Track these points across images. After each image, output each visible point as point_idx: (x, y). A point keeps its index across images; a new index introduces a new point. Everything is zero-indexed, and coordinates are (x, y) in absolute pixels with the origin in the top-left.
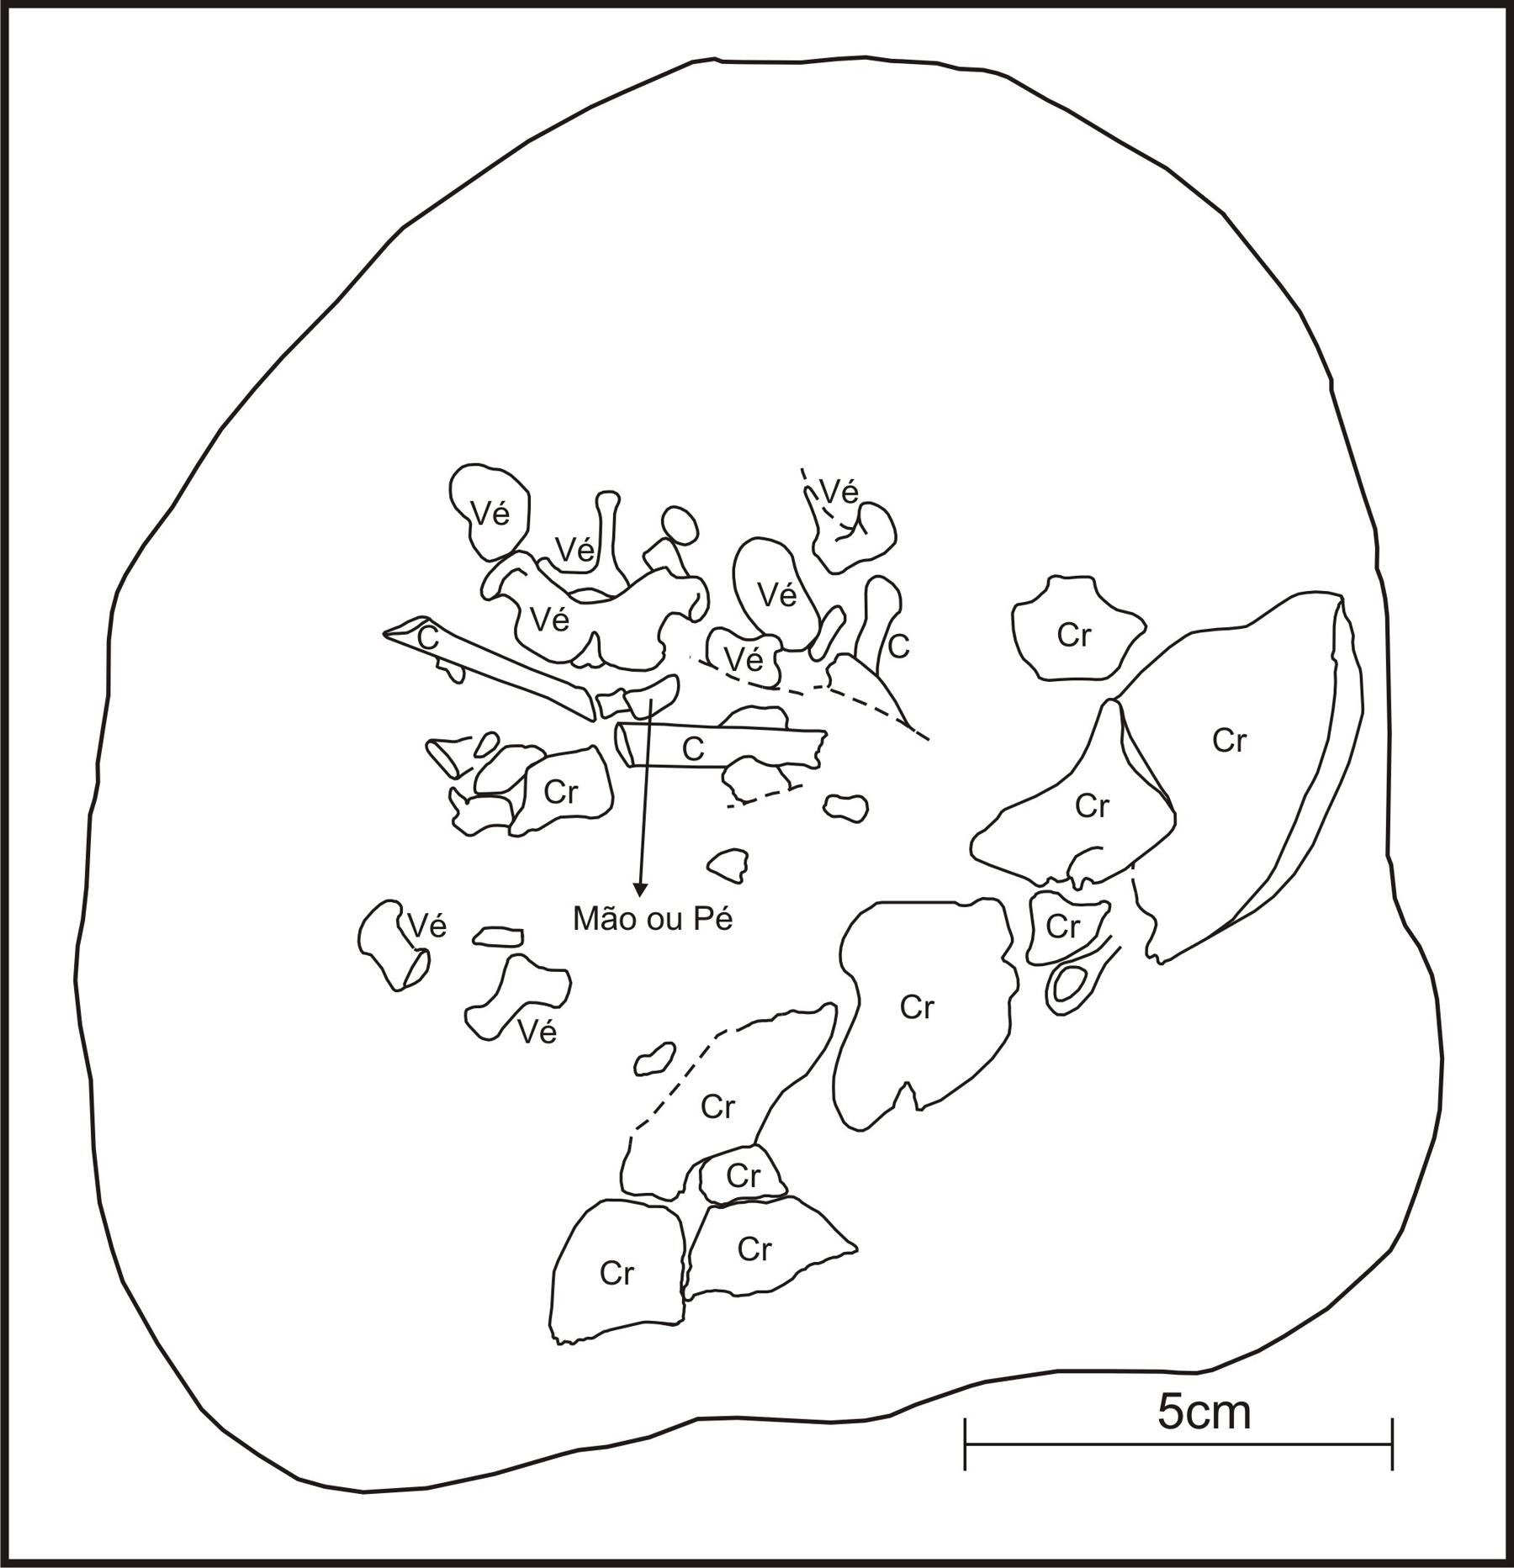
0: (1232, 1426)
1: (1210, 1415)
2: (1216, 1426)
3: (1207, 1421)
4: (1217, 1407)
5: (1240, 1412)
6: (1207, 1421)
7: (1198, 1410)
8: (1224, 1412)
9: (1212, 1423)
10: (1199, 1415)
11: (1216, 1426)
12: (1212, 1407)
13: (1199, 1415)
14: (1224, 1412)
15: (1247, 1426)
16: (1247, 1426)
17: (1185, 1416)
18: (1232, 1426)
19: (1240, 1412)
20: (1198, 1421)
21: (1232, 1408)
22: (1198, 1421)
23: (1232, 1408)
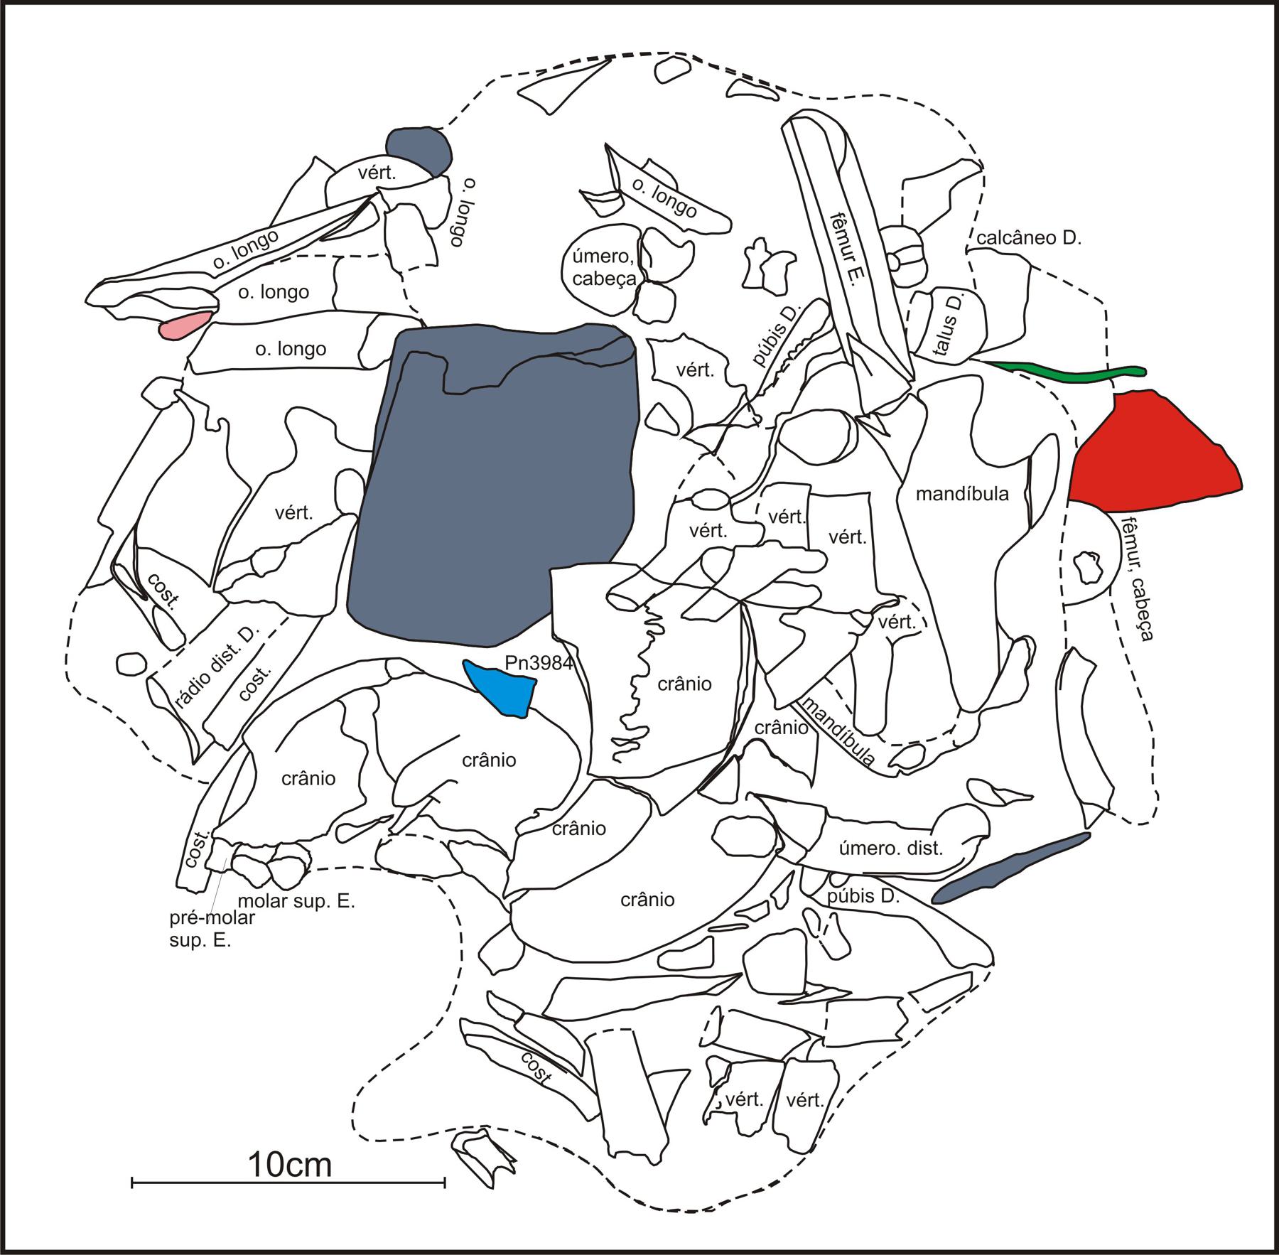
1: (303, 1167)
4: (308, 1161)
5: (324, 1165)
7: (294, 1163)
8: (313, 1165)
10: (295, 1167)
13: (295, 1167)
14: (313, 1165)
19: (324, 1165)
20: (294, 1171)
22: (294, 1171)
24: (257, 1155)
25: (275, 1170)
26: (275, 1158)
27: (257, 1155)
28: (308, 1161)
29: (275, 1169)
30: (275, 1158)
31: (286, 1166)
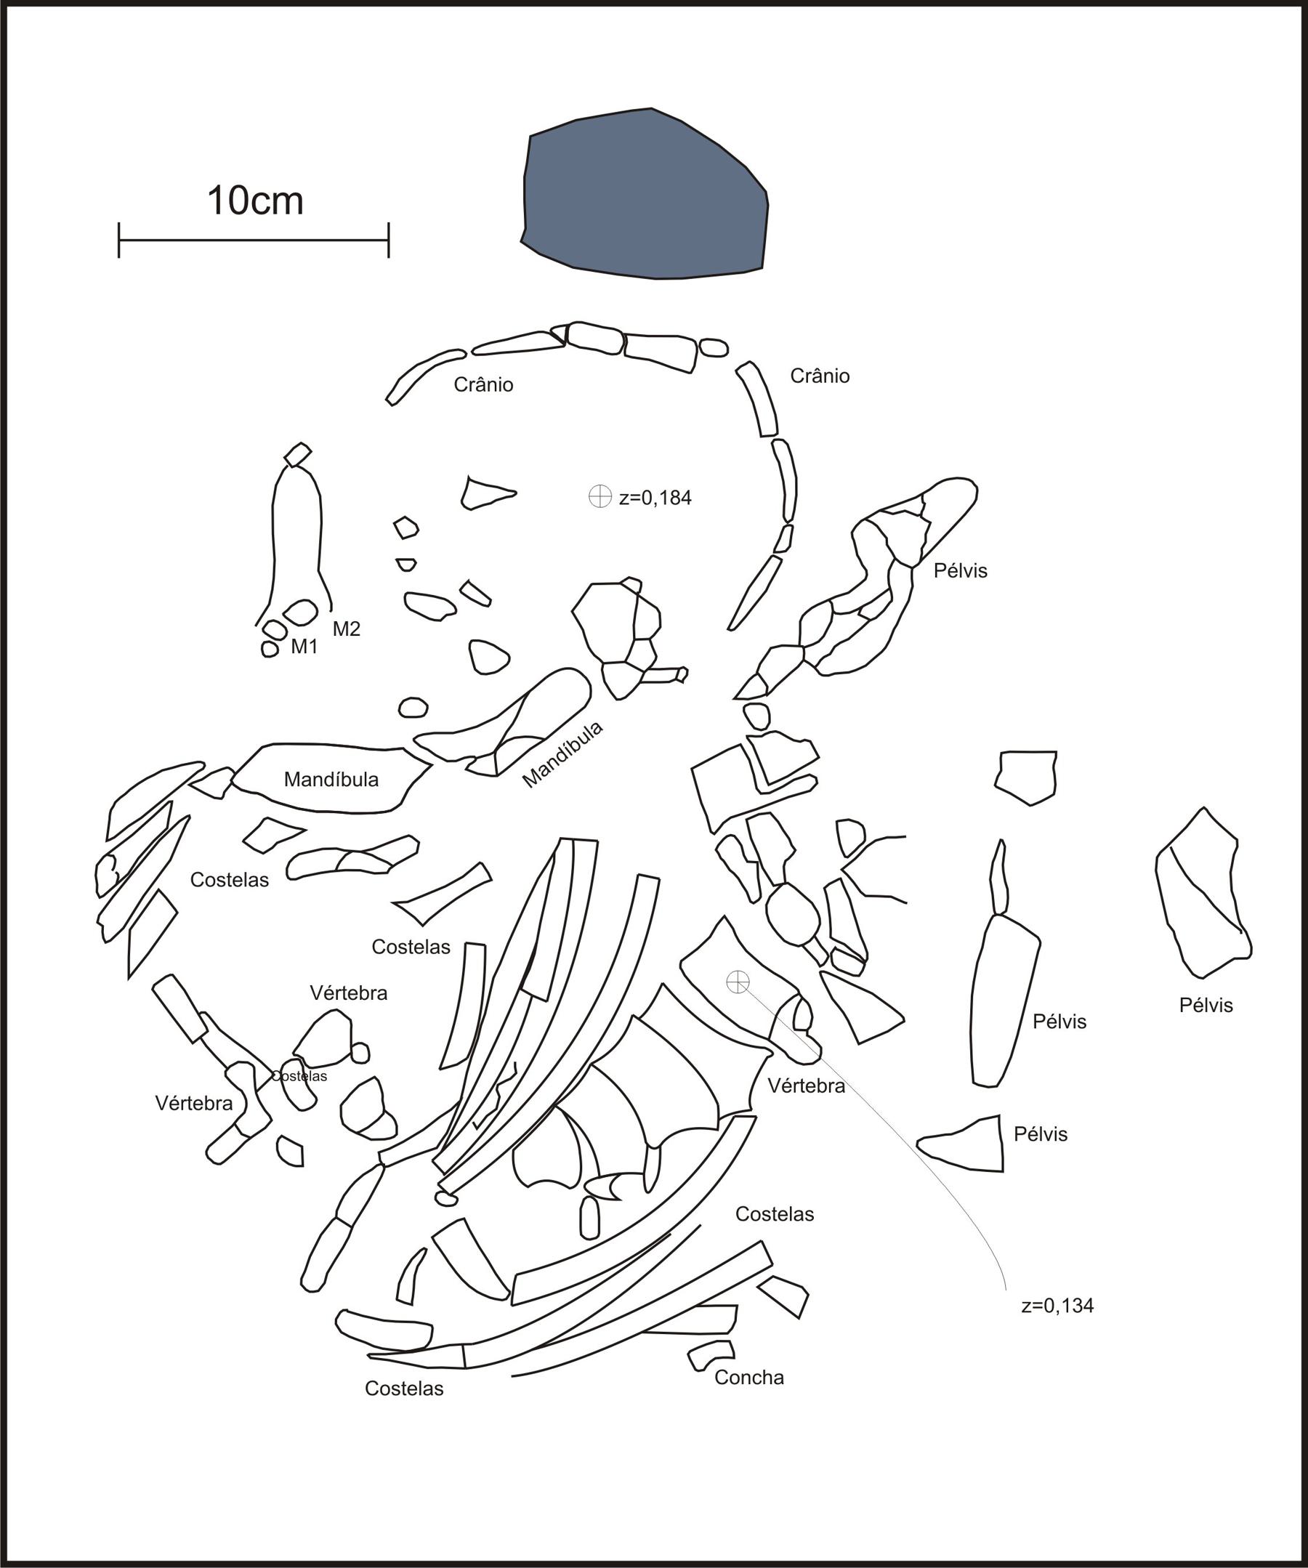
0: (288, 212)
1: (270, 203)
2: (275, 212)
3: (268, 208)
4: (276, 197)
5: (294, 200)
6: (268, 208)
7: (260, 199)
8: (282, 200)
9: (272, 210)
10: (262, 204)
11: (275, 212)
12: (272, 197)
14: (282, 200)
15: (300, 212)
16: (300, 212)
17: (251, 202)
18: (288, 212)
19: (294, 200)
20: (261, 207)
21: (288, 198)
22: (261, 207)
23: (288, 198)
24: (217, 189)
25: (239, 205)
26: (239, 194)
27: (217, 189)
28: (276, 197)
29: (239, 205)
30: (239, 192)
31: (251, 202)
